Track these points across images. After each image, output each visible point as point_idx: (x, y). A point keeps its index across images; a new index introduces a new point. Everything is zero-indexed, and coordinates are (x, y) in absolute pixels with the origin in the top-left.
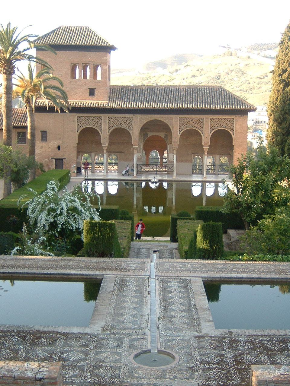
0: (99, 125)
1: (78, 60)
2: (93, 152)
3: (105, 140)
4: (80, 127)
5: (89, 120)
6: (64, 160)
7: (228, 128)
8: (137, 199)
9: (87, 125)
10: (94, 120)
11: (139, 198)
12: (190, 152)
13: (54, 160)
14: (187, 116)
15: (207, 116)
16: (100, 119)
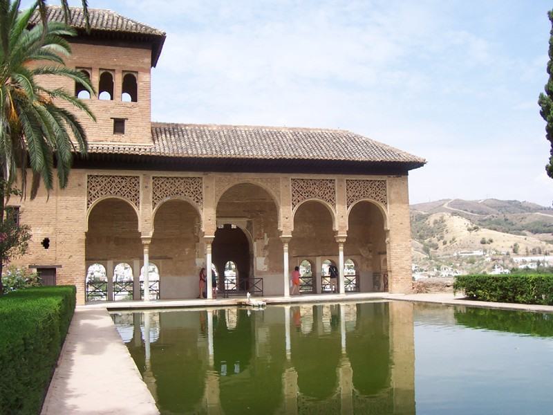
0: (133, 194)
1: (90, 61)
2: (110, 259)
3: (146, 228)
4: (93, 198)
5: (111, 186)
6: (58, 270)
7: (378, 198)
10: (123, 184)
13: (35, 271)
14: (306, 176)
15: (341, 176)
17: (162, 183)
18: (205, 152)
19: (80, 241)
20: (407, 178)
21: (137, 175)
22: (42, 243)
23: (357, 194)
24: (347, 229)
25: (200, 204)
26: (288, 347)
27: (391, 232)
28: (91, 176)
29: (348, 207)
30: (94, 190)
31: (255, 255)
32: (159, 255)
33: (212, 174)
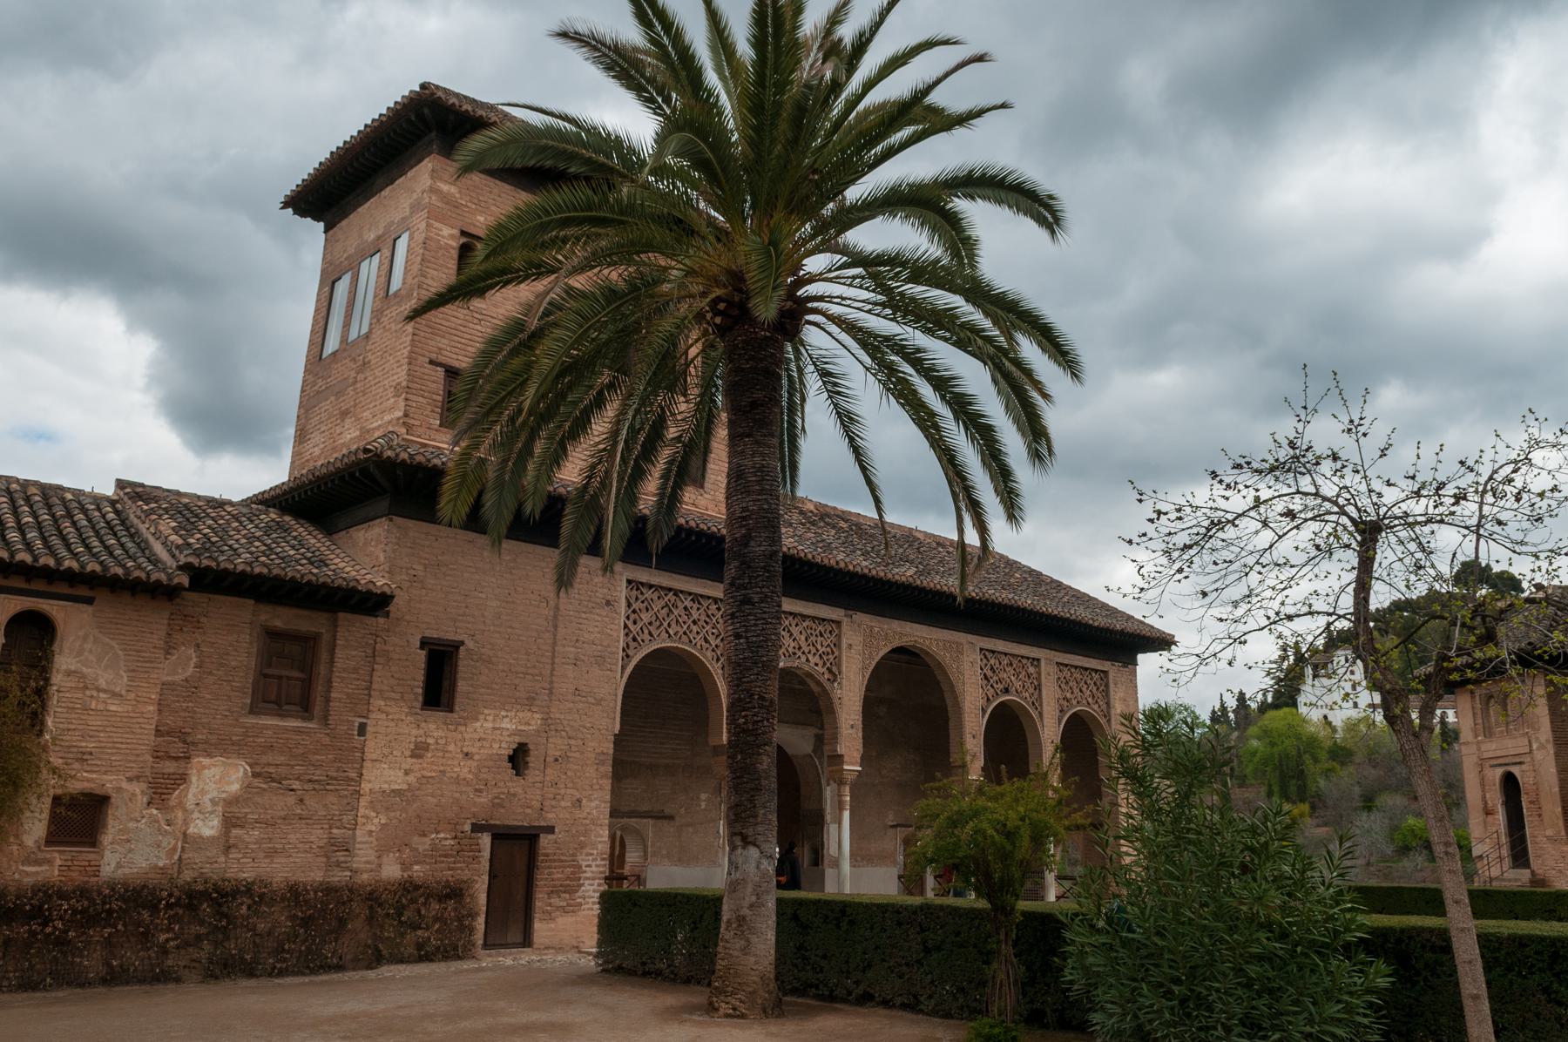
9: (664, 635)
12: (891, 819)
13: (486, 840)
14: (1000, 645)
20: (1135, 672)
22: (512, 759)
32: (645, 807)
33: (860, 617)
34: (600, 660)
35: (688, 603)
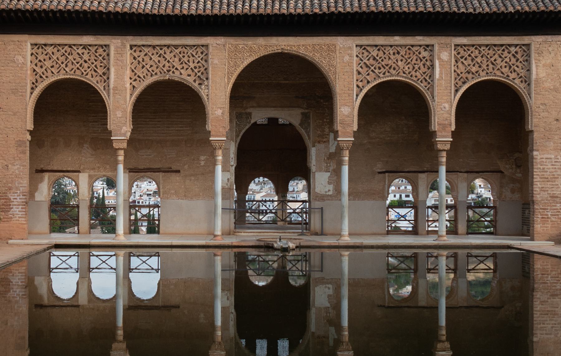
0: (100, 71)
4: (39, 80)
8: (223, 308)
9: (63, 72)
10: (86, 57)
11: (228, 308)
14: (380, 40)
16: (105, 54)
17: (146, 55)
18: (209, 6)
19: (20, 143)
21: (107, 42)
23: (474, 69)
24: (453, 128)
25: (203, 87)
26: (345, 323)
27: (536, 135)
28: (36, 45)
29: (457, 91)
30: (41, 67)
31: (313, 169)
34: (14, 91)
35: (80, 51)
